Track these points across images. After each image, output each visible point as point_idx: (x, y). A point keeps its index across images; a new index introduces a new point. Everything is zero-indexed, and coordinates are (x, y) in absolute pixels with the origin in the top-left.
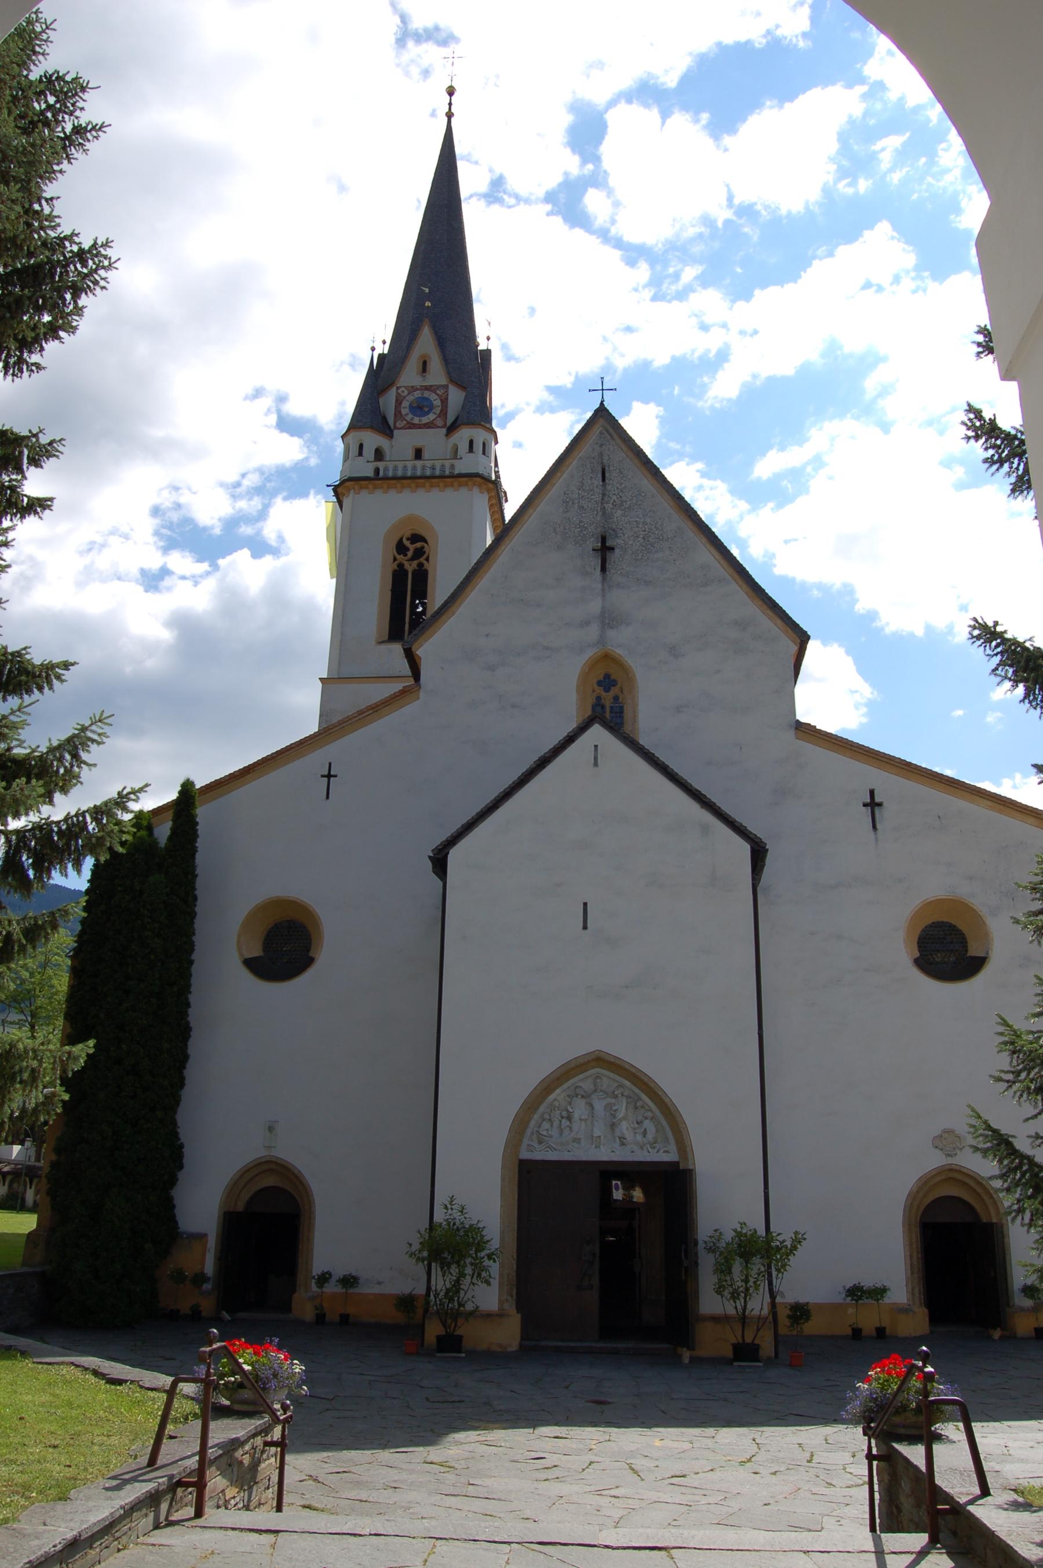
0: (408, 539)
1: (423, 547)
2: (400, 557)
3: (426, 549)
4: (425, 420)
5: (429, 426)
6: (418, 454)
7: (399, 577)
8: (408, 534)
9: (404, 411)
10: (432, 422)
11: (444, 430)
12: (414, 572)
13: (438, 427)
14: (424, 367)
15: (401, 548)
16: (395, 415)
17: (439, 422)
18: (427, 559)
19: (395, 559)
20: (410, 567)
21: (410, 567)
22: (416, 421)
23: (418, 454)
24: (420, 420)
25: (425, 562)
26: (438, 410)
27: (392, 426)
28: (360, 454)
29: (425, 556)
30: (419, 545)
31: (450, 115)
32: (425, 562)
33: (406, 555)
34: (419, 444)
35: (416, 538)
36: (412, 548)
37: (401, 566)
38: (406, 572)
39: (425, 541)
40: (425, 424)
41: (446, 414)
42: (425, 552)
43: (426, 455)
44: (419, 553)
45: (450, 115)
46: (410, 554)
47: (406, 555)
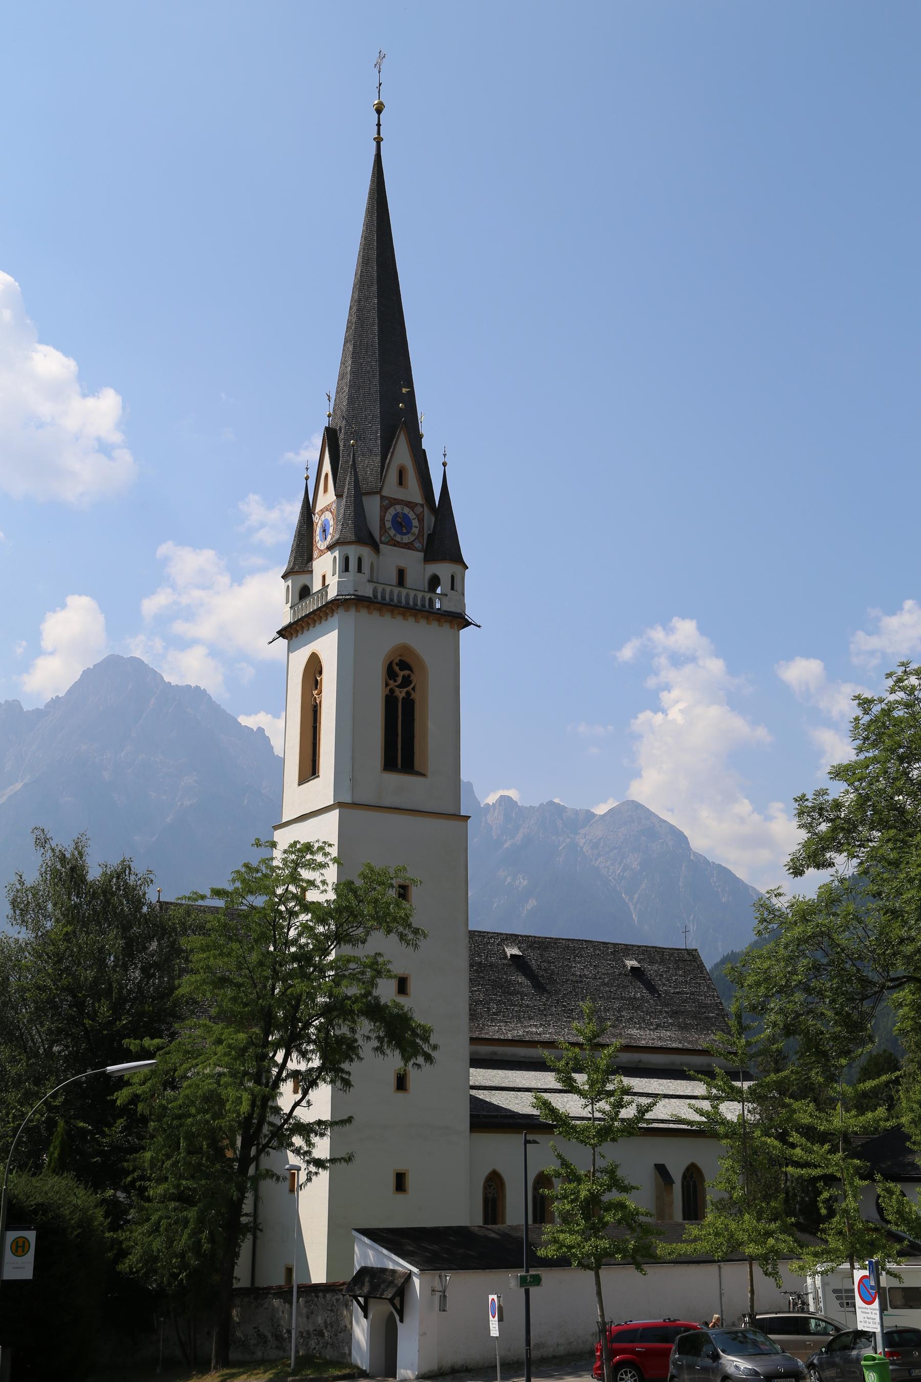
0: (397, 664)
1: (409, 676)
2: (391, 682)
3: (413, 677)
4: (406, 539)
5: (408, 546)
6: (401, 573)
7: (390, 701)
8: (397, 661)
9: (388, 525)
10: (411, 543)
11: (421, 555)
12: (403, 698)
13: (417, 550)
14: (401, 482)
15: (391, 673)
16: (381, 528)
17: (417, 545)
18: (413, 689)
19: (387, 685)
20: (401, 694)
21: (401, 694)
22: (398, 538)
23: (401, 573)
24: (402, 539)
25: (412, 692)
26: (416, 531)
27: (378, 541)
28: (360, 570)
29: (412, 686)
30: (397, 668)
31: (378, 141)
32: (412, 692)
33: (395, 681)
34: (402, 564)
35: (404, 665)
36: (401, 674)
37: (392, 691)
38: (396, 698)
39: (410, 669)
40: (406, 544)
41: (423, 536)
42: (411, 682)
43: (410, 580)
44: (407, 682)
45: (378, 141)
46: (399, 680)
47: (395, 681)
